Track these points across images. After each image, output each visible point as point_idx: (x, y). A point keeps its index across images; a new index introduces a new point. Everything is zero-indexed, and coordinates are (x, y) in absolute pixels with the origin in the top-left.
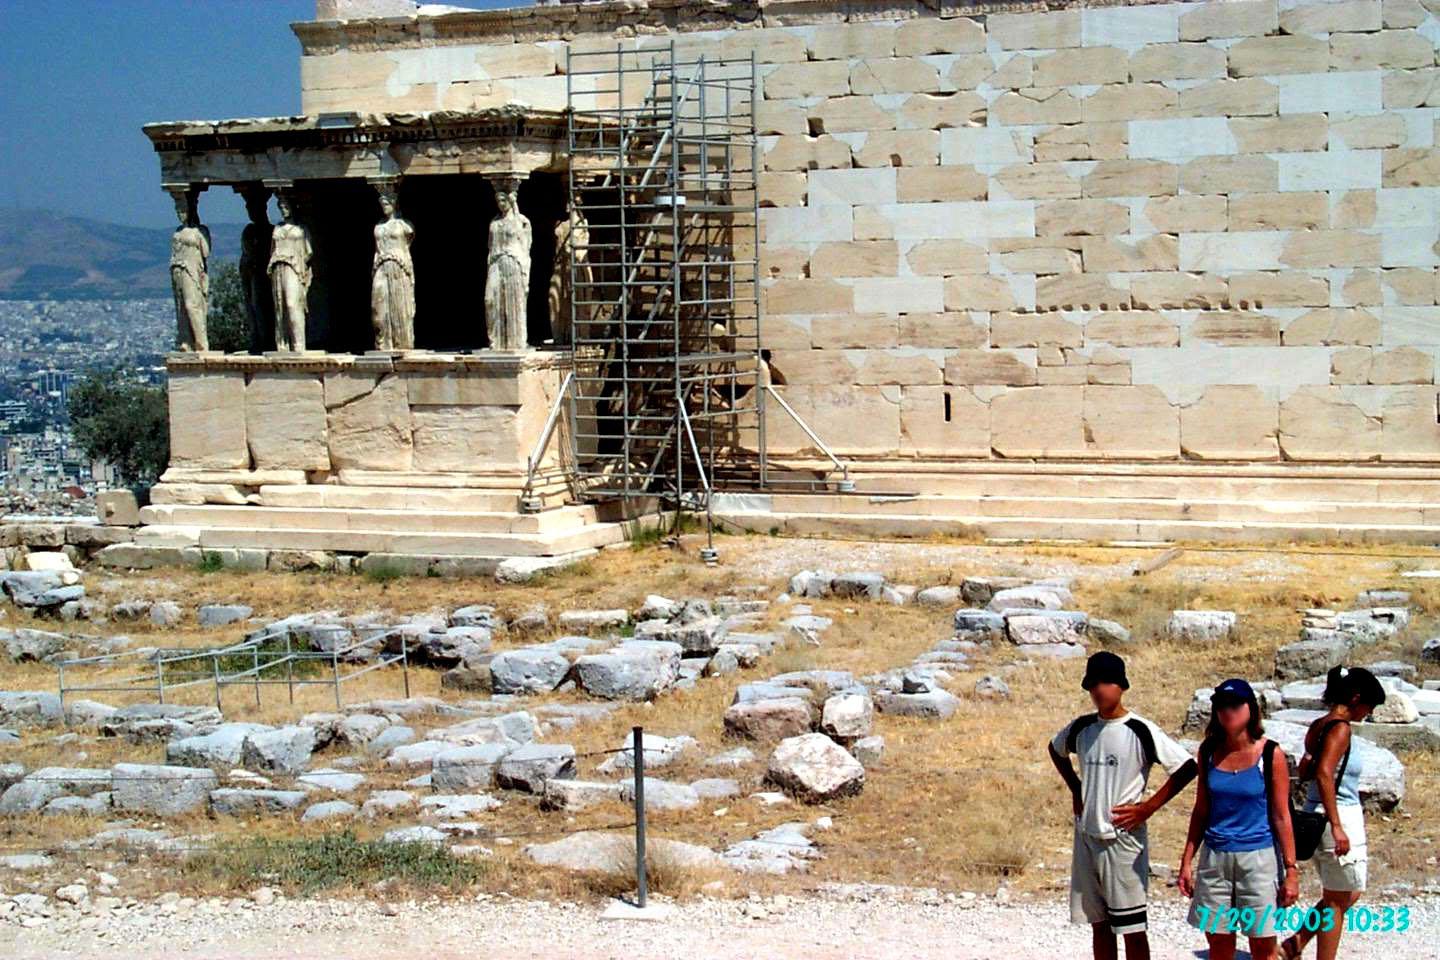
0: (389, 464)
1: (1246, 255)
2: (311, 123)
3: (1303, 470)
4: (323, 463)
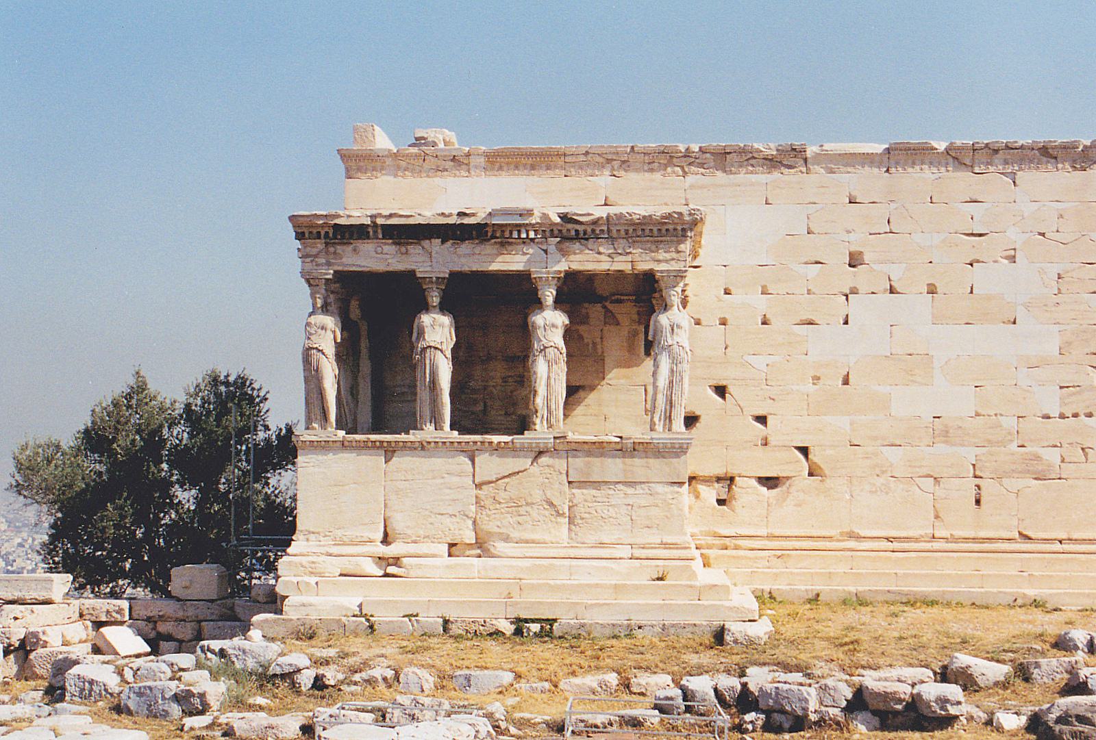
0: (547, 538)
4: (470, 537)
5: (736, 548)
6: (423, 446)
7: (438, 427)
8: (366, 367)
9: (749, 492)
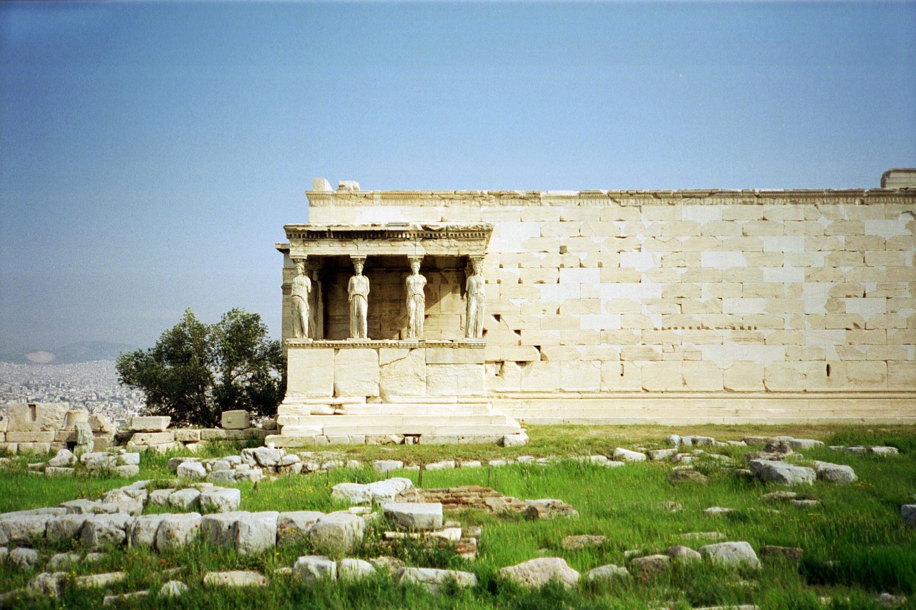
0: (415, 393)
1: (749, 308)
2: (383, 228)
3: (776, 395)
4: (376, 393)
5: (506, 397)
6: (354, 346)
7: (361, 336)
8: (321, 304)
9: (511, 368)
